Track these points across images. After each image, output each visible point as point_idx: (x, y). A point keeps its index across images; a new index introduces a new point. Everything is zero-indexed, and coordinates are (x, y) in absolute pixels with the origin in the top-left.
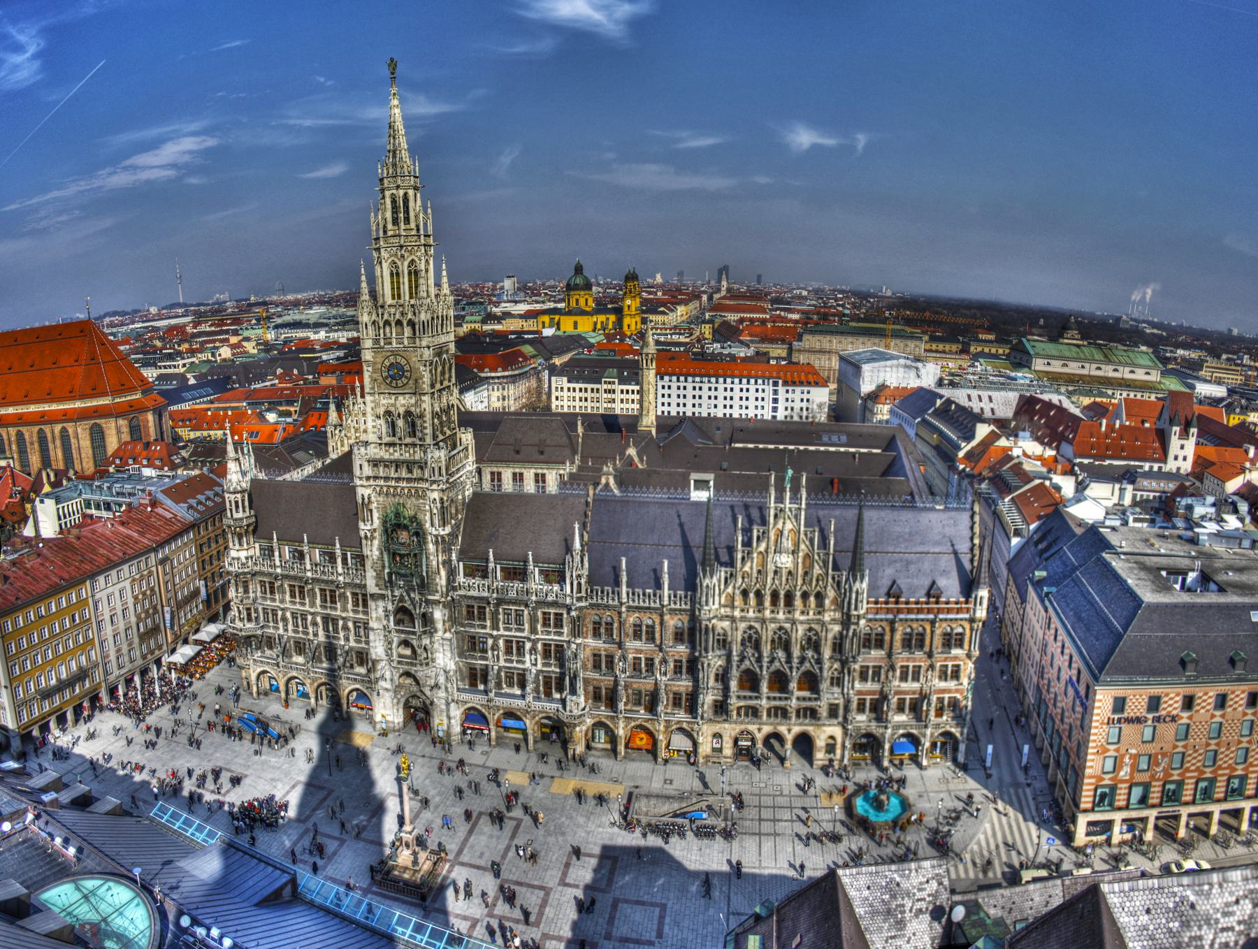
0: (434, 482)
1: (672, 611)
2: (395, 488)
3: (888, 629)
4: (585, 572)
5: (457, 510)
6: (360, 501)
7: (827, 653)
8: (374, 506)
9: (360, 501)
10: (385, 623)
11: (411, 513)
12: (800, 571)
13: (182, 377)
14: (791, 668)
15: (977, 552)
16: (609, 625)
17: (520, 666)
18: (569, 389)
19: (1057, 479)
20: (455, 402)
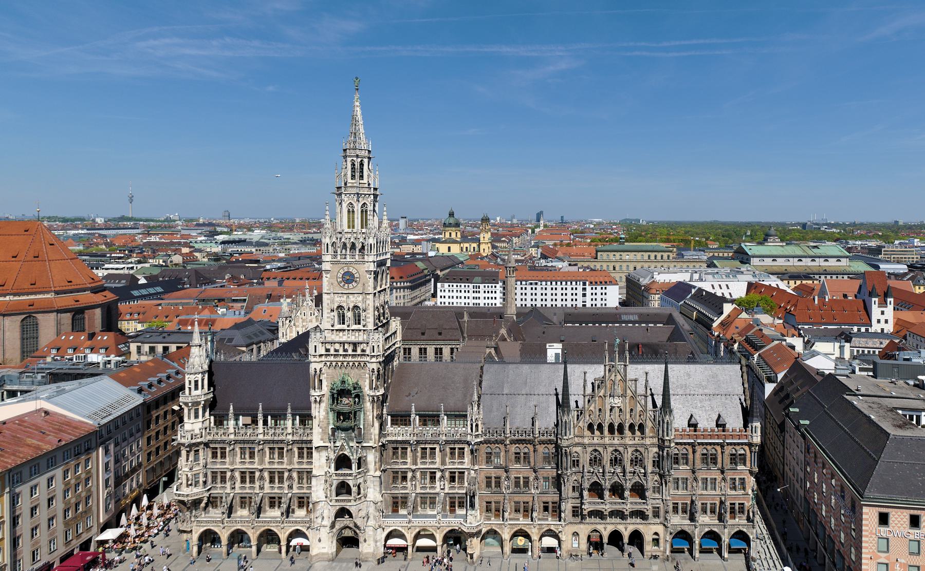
0: (373, 356)
1: (542, 442)
2: (342, 362)
3: (690, 450)
9: (312, 371)
10: (326, 469)
12: (628, 410)
14: (626, 480)
17: (431, 491)
19: (790, 340)
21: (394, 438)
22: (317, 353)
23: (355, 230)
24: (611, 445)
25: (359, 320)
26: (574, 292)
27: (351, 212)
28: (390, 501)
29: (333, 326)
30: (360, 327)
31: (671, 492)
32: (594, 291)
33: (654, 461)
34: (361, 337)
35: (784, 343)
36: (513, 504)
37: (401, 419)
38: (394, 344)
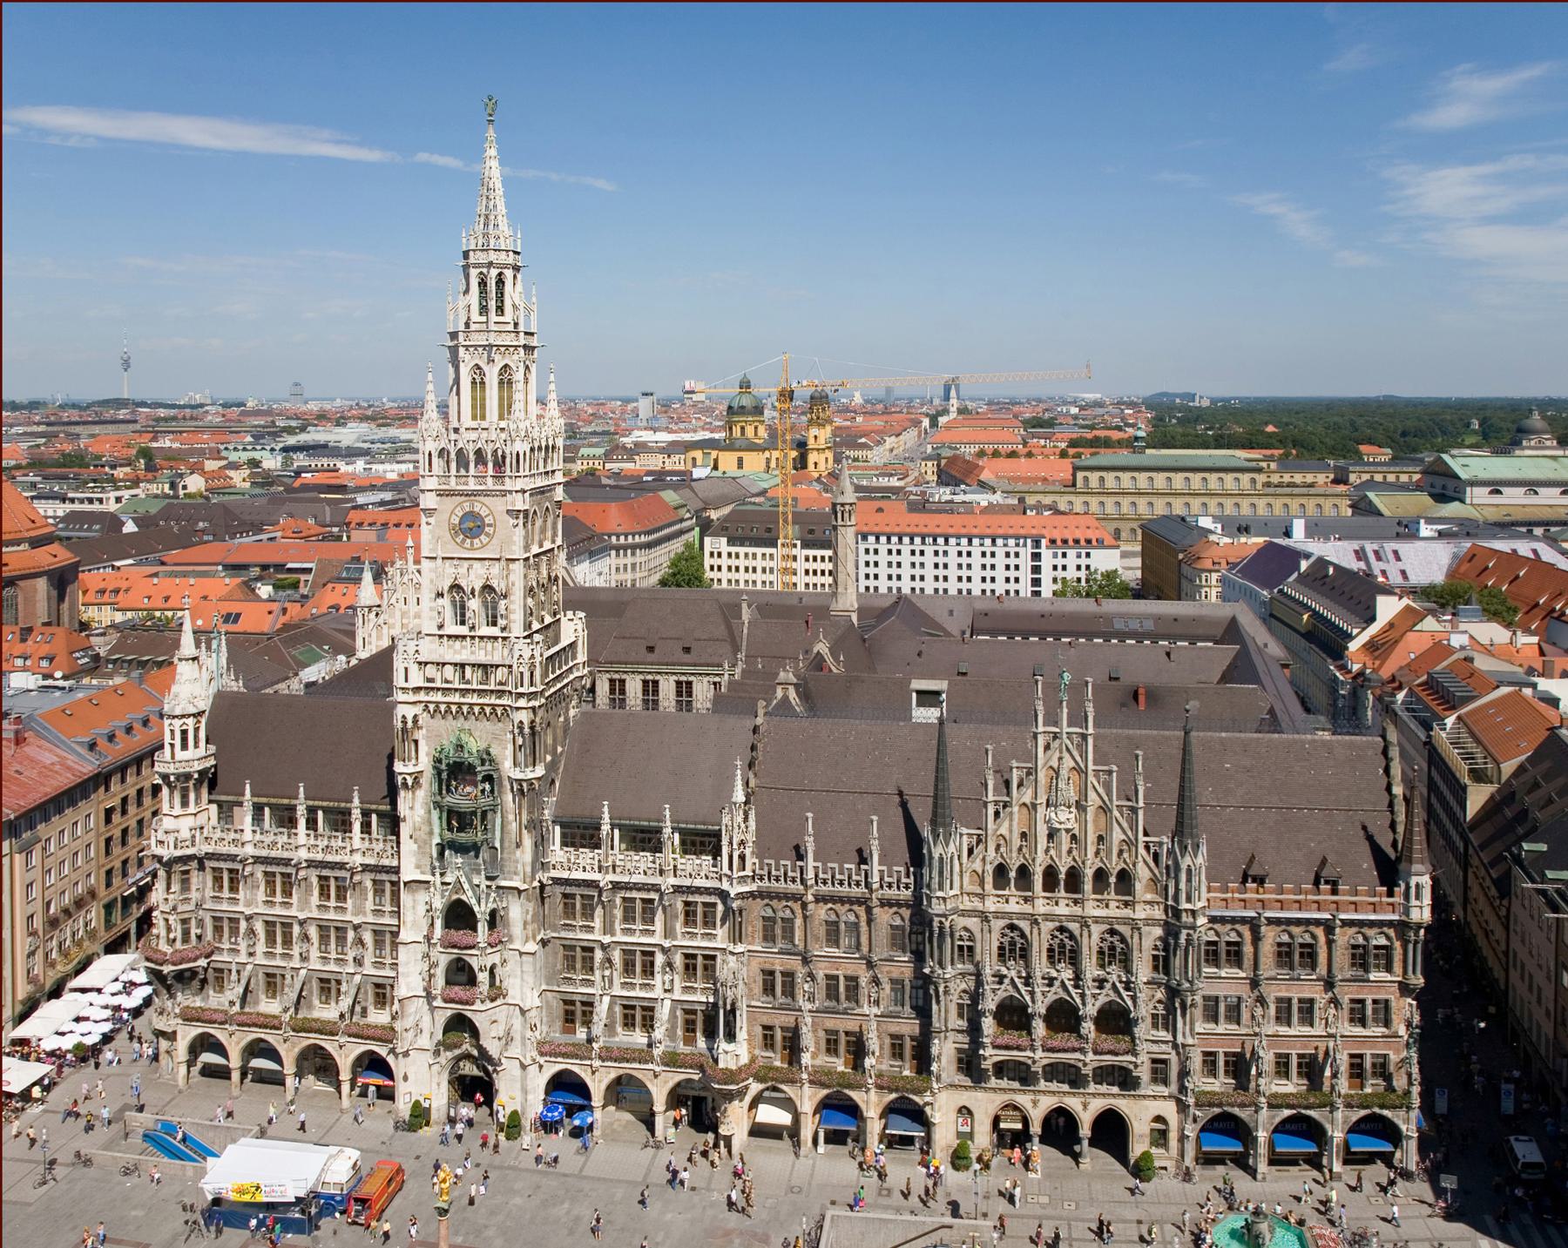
2: (460, 705)
4: (751, 838)
5: (555, 740)
6: (400, 725)
8: (420, 735)
11: (483, 746)
12: (1092, 837)
13: (114, 522)
16: (788, 924)
18: (730, 555)
20: (561, 573)
21: (565, 875)
23: (484, 424)
27: (479, 384)
28: (559, 1009)
30: (495, 631)
32: (1060, 561)
33: (1155, 958)
34: (496, 654)
36: (822, 1034)
37: (582, 834)
38: (570, 670)
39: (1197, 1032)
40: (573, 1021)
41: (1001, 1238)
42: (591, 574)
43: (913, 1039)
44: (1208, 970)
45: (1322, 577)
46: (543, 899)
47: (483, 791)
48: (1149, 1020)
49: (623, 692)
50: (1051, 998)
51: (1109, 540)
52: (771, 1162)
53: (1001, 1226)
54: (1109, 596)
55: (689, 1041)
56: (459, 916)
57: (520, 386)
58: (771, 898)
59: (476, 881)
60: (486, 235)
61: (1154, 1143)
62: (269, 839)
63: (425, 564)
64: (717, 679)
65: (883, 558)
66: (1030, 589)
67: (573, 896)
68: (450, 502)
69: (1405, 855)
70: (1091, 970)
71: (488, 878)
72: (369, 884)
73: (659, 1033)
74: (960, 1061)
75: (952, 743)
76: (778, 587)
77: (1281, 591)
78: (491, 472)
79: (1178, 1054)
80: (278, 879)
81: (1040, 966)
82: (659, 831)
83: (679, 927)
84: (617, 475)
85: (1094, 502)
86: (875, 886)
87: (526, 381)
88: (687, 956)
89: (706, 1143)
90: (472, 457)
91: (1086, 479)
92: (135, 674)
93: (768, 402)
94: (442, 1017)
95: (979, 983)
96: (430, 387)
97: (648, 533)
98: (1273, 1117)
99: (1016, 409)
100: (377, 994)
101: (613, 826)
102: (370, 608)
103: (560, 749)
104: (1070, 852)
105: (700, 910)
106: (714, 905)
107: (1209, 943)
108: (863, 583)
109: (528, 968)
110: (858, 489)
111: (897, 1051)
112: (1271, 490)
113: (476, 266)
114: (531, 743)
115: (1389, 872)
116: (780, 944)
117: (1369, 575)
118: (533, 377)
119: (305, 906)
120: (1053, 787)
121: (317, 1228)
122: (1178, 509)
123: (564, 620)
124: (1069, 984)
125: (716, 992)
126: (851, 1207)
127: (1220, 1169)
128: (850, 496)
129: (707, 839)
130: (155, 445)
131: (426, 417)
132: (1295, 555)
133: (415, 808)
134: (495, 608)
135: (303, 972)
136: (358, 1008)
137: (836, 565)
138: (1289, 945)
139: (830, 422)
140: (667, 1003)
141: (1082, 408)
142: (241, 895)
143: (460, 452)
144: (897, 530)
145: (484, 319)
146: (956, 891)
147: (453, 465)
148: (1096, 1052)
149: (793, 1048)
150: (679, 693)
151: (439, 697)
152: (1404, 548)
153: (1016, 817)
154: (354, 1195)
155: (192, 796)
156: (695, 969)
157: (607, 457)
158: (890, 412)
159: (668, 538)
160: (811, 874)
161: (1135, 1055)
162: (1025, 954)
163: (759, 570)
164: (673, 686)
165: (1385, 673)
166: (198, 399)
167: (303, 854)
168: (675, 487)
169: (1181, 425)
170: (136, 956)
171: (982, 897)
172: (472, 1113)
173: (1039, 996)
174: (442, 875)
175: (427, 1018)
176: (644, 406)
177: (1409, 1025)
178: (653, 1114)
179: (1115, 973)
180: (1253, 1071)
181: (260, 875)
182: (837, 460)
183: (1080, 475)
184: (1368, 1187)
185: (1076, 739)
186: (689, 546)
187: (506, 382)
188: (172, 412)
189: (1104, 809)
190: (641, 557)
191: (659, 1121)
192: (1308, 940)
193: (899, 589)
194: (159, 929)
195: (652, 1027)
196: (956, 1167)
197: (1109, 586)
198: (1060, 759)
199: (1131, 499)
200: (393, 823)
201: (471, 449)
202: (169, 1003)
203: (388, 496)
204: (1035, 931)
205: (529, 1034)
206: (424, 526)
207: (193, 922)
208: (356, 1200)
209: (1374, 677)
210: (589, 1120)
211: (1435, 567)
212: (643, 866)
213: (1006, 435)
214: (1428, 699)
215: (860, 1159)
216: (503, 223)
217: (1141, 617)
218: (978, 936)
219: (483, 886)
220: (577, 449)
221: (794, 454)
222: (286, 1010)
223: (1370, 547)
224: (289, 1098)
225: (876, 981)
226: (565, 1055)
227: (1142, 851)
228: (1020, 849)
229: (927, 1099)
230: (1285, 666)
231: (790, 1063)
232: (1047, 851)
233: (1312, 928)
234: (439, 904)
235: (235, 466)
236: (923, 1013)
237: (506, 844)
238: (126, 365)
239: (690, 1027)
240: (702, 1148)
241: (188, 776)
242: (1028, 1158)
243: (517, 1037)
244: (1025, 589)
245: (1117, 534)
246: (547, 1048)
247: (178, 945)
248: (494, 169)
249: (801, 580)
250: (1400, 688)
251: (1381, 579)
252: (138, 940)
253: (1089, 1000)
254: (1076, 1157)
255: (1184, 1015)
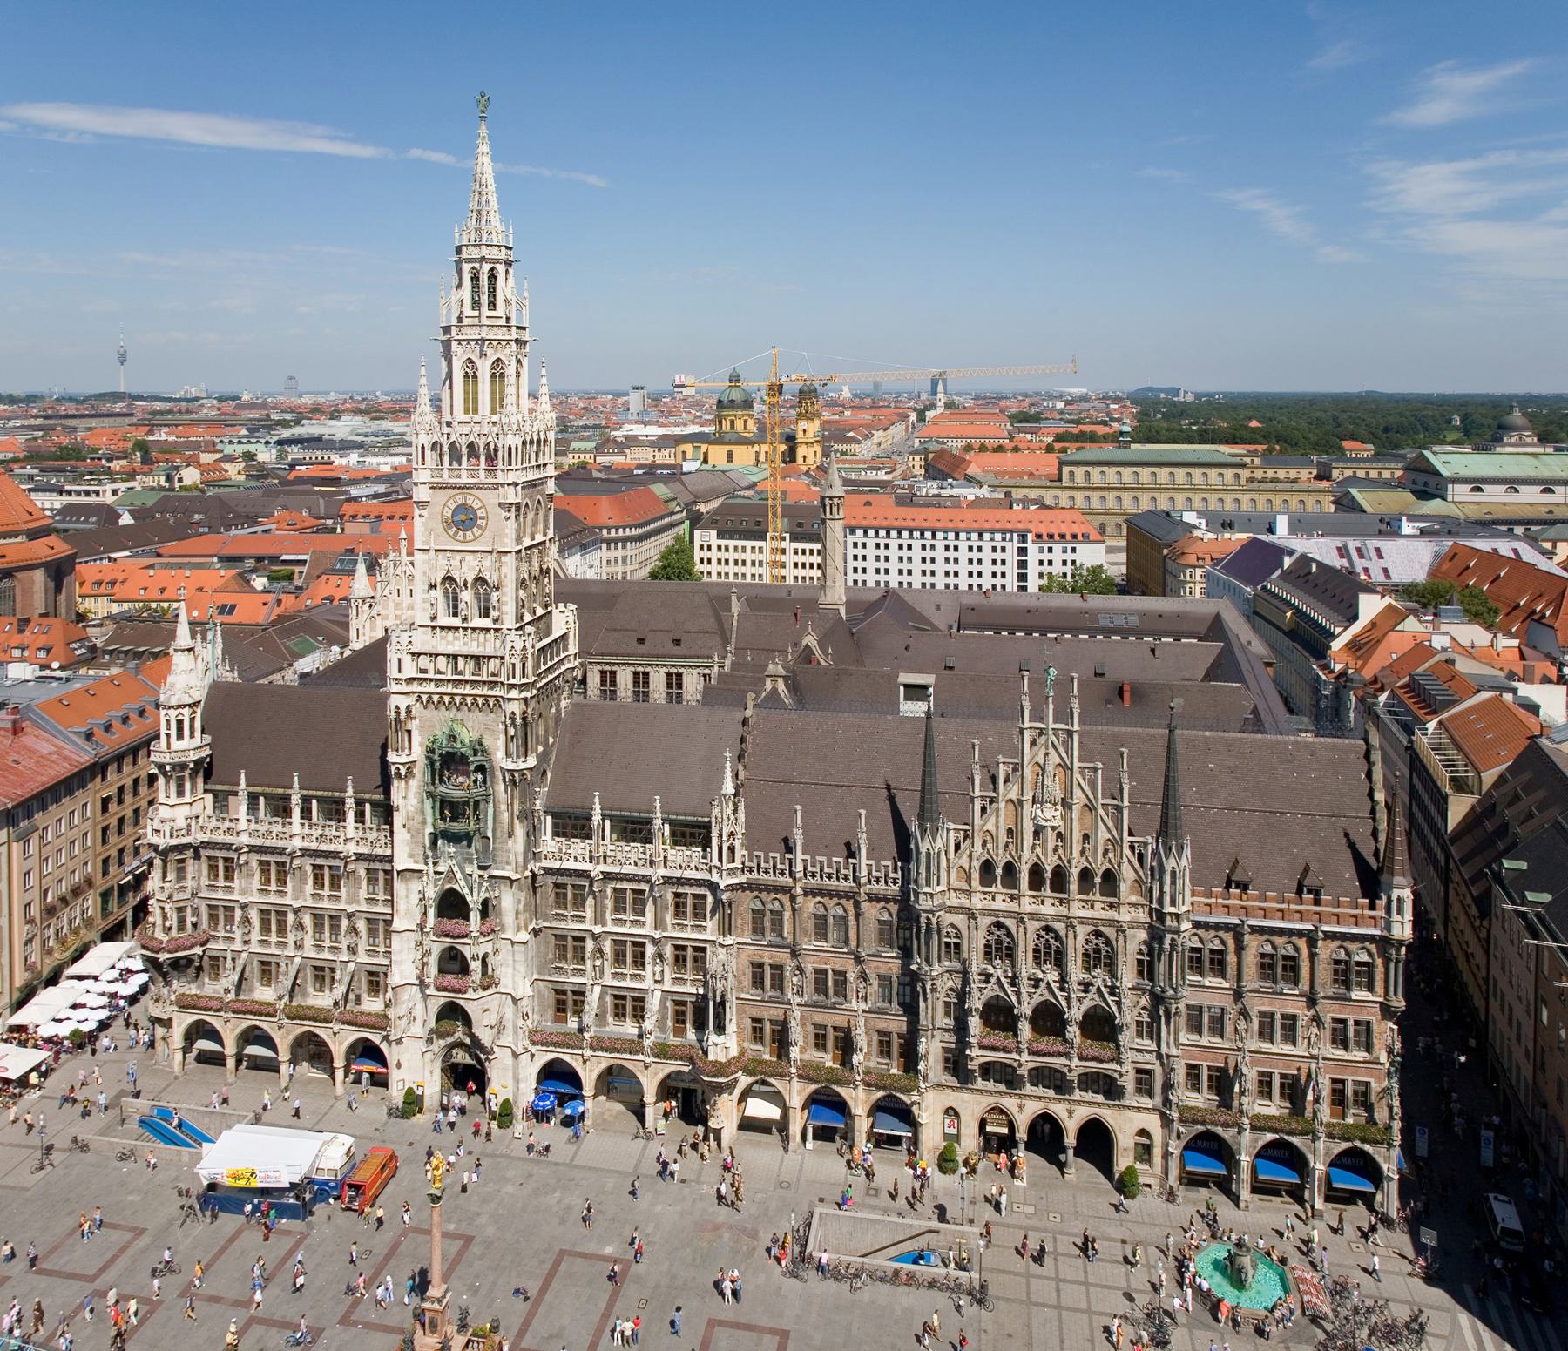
1: (874, 898)
2: (452, 696)
6: (393, 715)
7: (1128, 976)
11: (475, 736)
12: (1077, 836)
13: (110, 514)
15: (1382, 815)
16: (777, 916)
20: (553, 566)
21: (557, 865)
22: (404, 675)
23: (477, 418)
24: (1035, 916)
25: (487, 608)
26: (999, 556)
27: (471, 378)
28: (550, 998)
29: (433, 618)
30: (487, 623)
31: (1182, 1040)
33: (1140, 962)
35: (1508, 697)
36: (810, 1028)
37: (573, 824)
38: (561, 662)
39: (1180, 1042)
40: (564, 1011)
41: (987, 1247)
42: (582, 567)
43: (900, 1036)
44: (1192, 978)
45: (1306, 575)
46: (534, 888)
47: (475, 781)
48: (1134, 1027)
49: (613, 683)
50: (1037, 999)
51: (1094, 535)
52: (760, 1156)
53: (987, 1234)
54: (1094, 591)
55: (680, 1032)
56: (452, 905)
57: (512, 380)
58: (761, 891)
59: (468, 871)
60: (478, 230)
61: (1138, 1158)
62: (264, 828)
63: (418, 556)
64: (707, 671)
65: (871, 552)
66: (1016, 584)
67: (564, 886)
68: (442, 495)
69: (1386, 866)
70: (1076, 973)
71: (480, 868)
72: (363, 873)
73: (649, 1024)
74: (947, 1060)
75: (939, 738)
76: (767, 580)
77: (1264, 588)
78: (483, 465)
79: (1162, 1064)
80: (273, 868)
81: (1027, 966)
82: (649, 822)
83: (669, 918)
84: (607, 469)
85: (1079, 497)
86: (863, 881)
87: (518, 375)
88: (677, 947)
89: (696, 1136)
90: (464, 450)
91: (1072, 474)
92: (132, 664)
93: (757, 396)
94: (435, 1005)
95: (966, 981)
96: (423, 381)
97: (639, 526)
98: (1256, 1140)
99: (1002, 403)
100: (371, 982)
101: (604, 817)
102: (364, 599)
103: (551, 740)
104: (1055, 850)
105: (690, 901)
106: (704, 897)
107: (1193, 950)
108: (851, 576)
109: (520, 957)
110: (846, 482)
111: (884, 1049)
112: (1255, 486)
113: (469, 261)
114: (523, 733)
115: (1372, 884)
116: (769, 937)
117: (1351, 572)
118: (525, 371)
119: (299, 894)
120: (1039, 784)
121: (312, 1213)
122: (1163, 504)
123: (555, 613)
124: (1055, 986)
125: (705, 984)
126: (839, 1206)
127: (1203, 1191)
128: (838, 490)
129: (697, 831)
130: (151, 438)
131: (419, 410)
132: (1279, 552)
133: (408, 798)
134: (487, 600)
135: (297, 960)
136: (352, 996)
137: (824, 559)
138: (1272, 956)
139: (819, 416)
140: (658, 994)
141: (1068, 403)
142: (236, 884)
143: (453, 446)
144: (885, 523)
145: (476, 313)
146: (943, 887)
147: (446, 458)
148: (1081, 1059)
149: (782, 1041)
150: (669, 685)
151: (431, 688)
152: (1387, 545)
153: (1002, 813)
154: (348, 1181)
155: (188, 786)
156: (685, 960)
157: (598, 450)
158: (878, 406)
159: (658, 531)
160: (799, 867)
161: (1120, 1063)
162: (1011, 954)
163: (748, 563)
164: (663, 678)
165: (1368, 673)
166: (194, 392)
167: (297, 843)
168: (666, 480)
169: (1166, 420)
170: (132, 943)
171: (969, 893)
172: (464, 1101)
173: (1024, 996)
174: (435, 864)
175: (420, 1007)
176: (635, 400)
177: (1390, 1052)
178: (643, 1105)
179: (1100, 977)
180: (1237, 1089)
181: (254, 864)
182: (826, 454)
183: (1066, 470)
184: (1349, 1230)
185: (1062, 736)
186: (679, 539)
187: (498, 376)
188: (168, 406)
189: (1090, 807)
190: (631, 549)
191: (650, 1112)
192: (1292, 953)
193: (887, 583)
194: (155, 917)
195: (642, 1017)
196: (943, 1170)
197: (1094, 582)
198: (1046, 755)
199: (1116, 494)
200: (386, 812)
201: (464, 442)
202: (165, 991)
203: (381, 489)
204: (1021, 930)
205: (521, 1022)
206: (417, 518)
207: (189, 910)
208: (350, 1186)
209: (1356, 677)
210: (581, 1109)
211: (1417, 566)
212: (633, 857)
213: (993, 429)
214: (1409, 702)
215: (848, 1157)
216: (495, 219)
217: (1126, 613)
218: (965, 933)
219: (475, 876)
220: (569, 442)
221: (783, 447)
222: (280, 998)
223: (1352, 544)
224: (284, 1085)
225: (863, 976)
226: (556, 1044)
227: (1127, 851)
228: (1006, 846)
229: (915, 1098)
230: (1269, 665)
231: (779, 1057)
232: (1033, 848)
233: (1294, 939)
234: (432, 893)
235: (230, 459)
236: (911, 1010)
237: (498, 834)
238: (123, 358)
239: (680, 1018)
240: (691, 1141)
241: (183, 766)
242: (1014, 1164)
243: (509, 1026)
244: (1012, 584)
245: (1103, 527)
246: (538, 1037)
247: (174, 933)
248: (486, 165)
249: (790, 573)
250: (1382, 689)
251: (1363, 577)
252: (134, 928)
253: (1074, 1003)
254: (1061, 1166)
255: (1168, 1024)
